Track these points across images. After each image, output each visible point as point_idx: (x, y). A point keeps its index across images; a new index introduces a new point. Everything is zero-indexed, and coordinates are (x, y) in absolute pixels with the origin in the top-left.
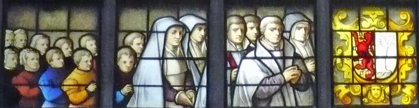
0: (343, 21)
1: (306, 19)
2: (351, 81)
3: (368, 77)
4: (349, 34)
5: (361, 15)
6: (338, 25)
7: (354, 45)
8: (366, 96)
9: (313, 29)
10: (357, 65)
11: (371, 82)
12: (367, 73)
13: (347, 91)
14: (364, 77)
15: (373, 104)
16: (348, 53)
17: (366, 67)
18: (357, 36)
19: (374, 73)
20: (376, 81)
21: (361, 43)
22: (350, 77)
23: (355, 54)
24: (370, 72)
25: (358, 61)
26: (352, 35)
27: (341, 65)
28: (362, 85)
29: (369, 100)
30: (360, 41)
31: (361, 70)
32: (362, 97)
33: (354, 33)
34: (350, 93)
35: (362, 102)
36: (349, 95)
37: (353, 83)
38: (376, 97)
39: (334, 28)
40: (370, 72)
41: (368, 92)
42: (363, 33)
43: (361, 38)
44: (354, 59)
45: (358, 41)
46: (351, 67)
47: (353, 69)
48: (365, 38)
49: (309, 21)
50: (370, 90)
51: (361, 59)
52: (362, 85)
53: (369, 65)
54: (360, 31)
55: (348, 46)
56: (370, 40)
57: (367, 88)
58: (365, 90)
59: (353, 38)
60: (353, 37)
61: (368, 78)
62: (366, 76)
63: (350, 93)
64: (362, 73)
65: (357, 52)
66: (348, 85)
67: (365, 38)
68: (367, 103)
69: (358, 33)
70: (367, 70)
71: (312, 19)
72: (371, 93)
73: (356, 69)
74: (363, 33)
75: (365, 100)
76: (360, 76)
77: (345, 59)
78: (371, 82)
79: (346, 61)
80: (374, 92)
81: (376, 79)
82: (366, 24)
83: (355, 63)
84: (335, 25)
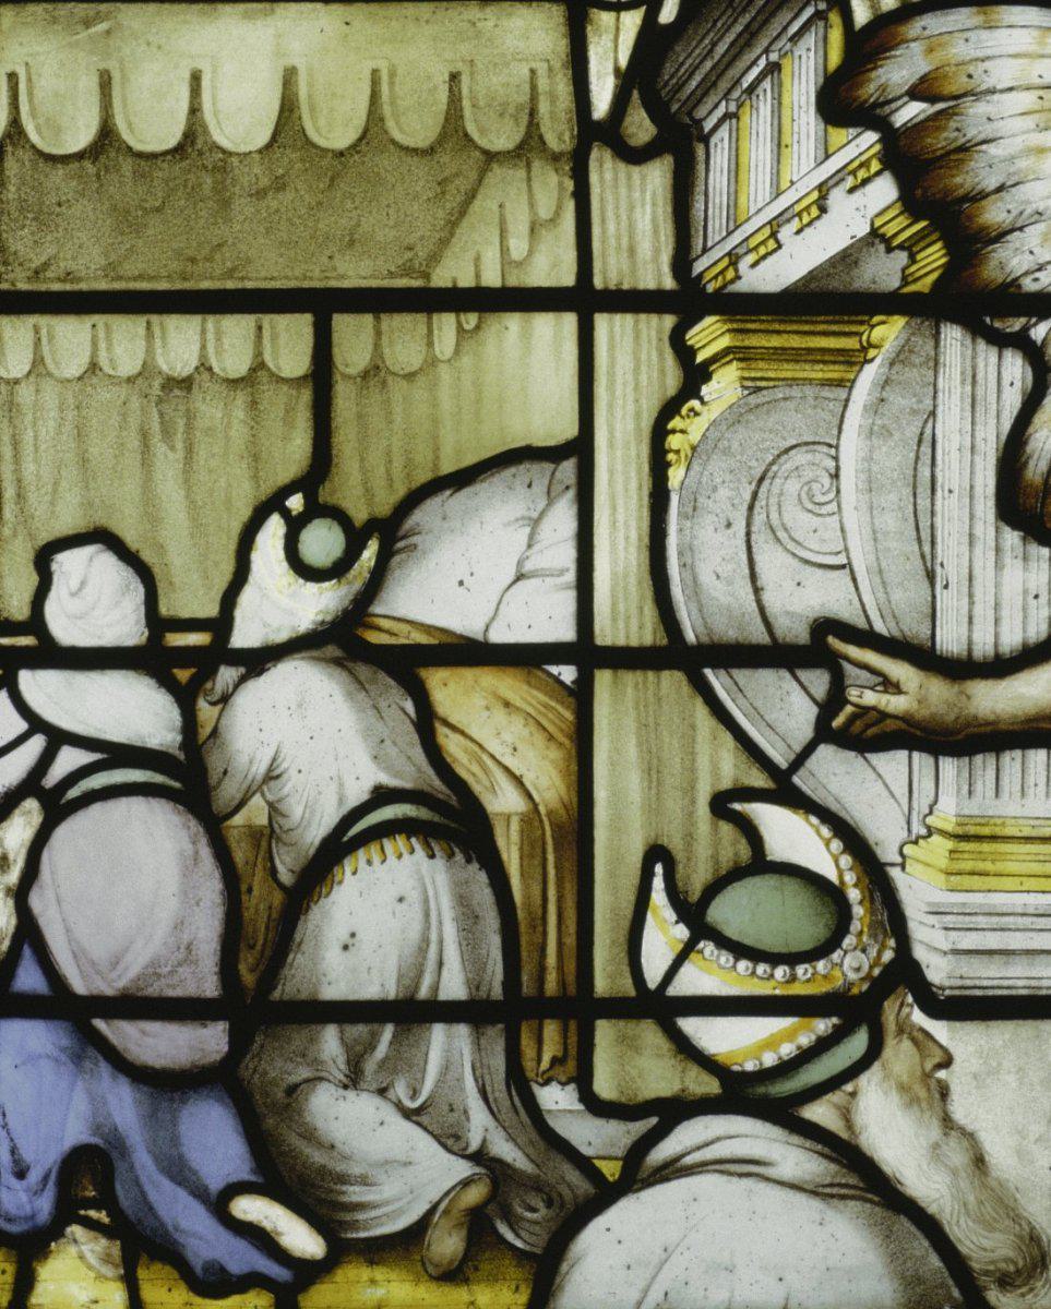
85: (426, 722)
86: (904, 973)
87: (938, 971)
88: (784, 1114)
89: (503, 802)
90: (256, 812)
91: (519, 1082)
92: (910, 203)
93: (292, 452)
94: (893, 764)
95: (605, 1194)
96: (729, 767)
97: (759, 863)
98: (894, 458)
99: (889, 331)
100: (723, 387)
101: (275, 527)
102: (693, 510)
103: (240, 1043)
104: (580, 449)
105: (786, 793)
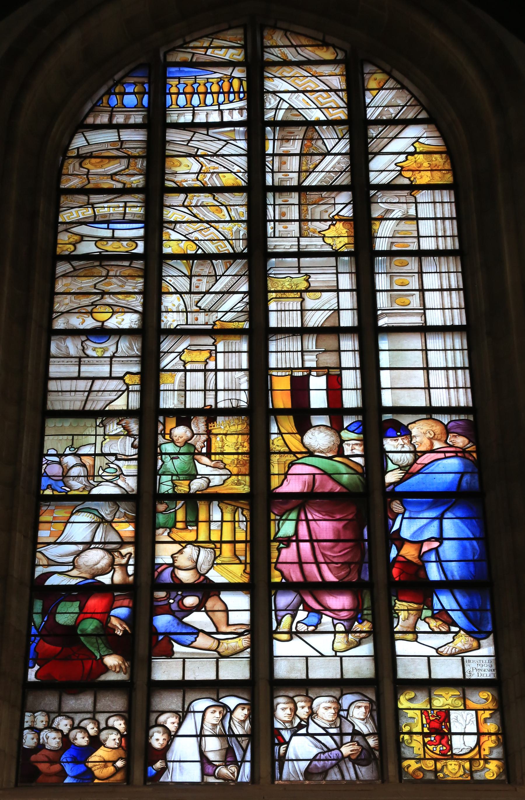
0: (410, 700)
1: (366, 699)
2: (422, 756)
3: (443, 752)
4: (419, 712)
5: (432, 694)
6: (403, 702)
7: (425, 722)
8: (442, 770)
9: (375, 707)
10: (429, 741)
11: (446, 757)
12: (441, 749)
13: (418, 765)
14: (438, 753)
15: (449, 778)
16: (418, 729)
17: (440, 743)
18: (429, 714)
19: (451, 748)
20: (453, 757)
21: (433, 720)
22: (421, 752)
23: (426, 730)
24: (444, 748)
25: (431, 737)
26: (422, 714)
27: (410, 741)
28: (436, 760)
29: (444, 775)
30: (431, 718)
31: (433, 746)
32: (436, 771)
33: (423, 711)
34: (421, 767)
35: (436, 777)
36: (420, 769)
37: (425, 759)
38: (454, 772)
39: (400, 706)
40: (444, 748)
41: (443, 767)
42: (435, 711)
43: (433, 716)
44: (424, 735)
45: (429, 719)
46: (422, 743)
47: (425, 744)
48: (437, 716)
49: (370, 701)
50: (446, 765)
51: (434, 736)
52: (436, 760)
53: (444, 741)
54: (431, 709)
55: (418, 723)
56: (443, 718)
57: (442, 763)
58: (439, 765)
59: (424, 716)
60: (424, 716)
61: (443, 754)
62: (440, 751)
63: (421, 767)
64: (435, 749)
65: (428, 729)
66: (419, 760)
67: (437, 716)
68: (442, 778)
69: (429, 711)
70: (441, 746)
71: (374, 698)
72: (447, 767)
73: (428, 745)
74: (435, 711)
75: (441, 775)
76: (432, 752)
77: (414, 735)
78: (446, 757)
79: (415, 737)
80: (450, 767)
81: (453, 754)
82: (438, 703)
83: (426, 740)
84: (402, 704)
85: (81, 460)
86: (122, 474)
87: (125, 474)
88: (111, 482)
89: (87, 464)
90: (66, 465)
91: (88, 480)
92: (124, 429)
93: (71, 444)
94: (122, 462)
95: (95, 487)
96: (107, 462)
97: (110, 467)
98: (122, 444)
99: (122, 437)
100: (108, 440)
101: (68, 448)
102: (105, 447)
103: (63, 478)
104: (95, 444)
105: (112, 463)
